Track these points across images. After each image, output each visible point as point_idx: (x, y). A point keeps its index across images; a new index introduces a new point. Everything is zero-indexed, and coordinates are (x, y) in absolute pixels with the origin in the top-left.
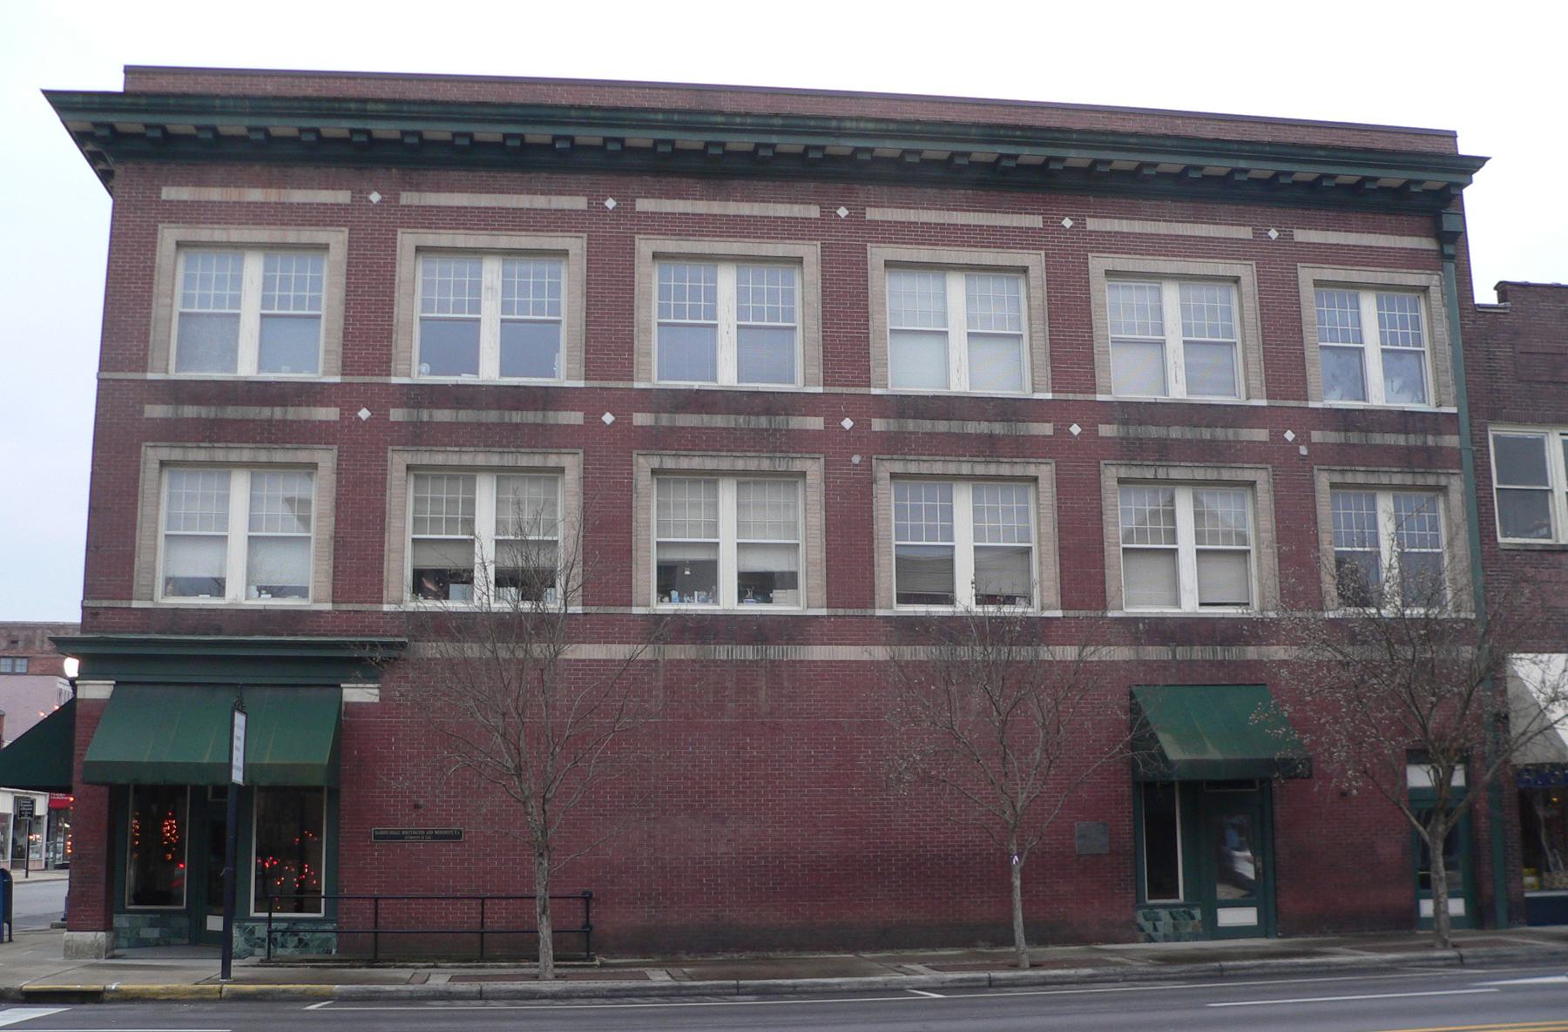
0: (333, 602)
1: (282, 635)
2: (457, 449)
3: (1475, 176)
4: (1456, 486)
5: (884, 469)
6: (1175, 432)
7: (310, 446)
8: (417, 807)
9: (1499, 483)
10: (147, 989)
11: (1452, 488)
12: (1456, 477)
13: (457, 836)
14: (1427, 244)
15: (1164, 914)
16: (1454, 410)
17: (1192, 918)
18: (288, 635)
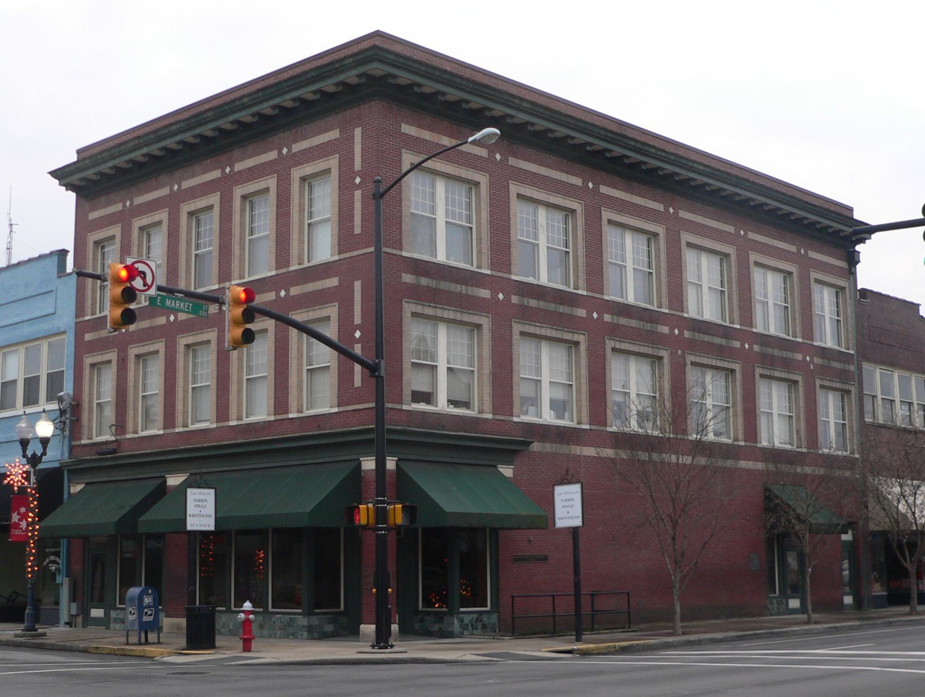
0: (493, 414)
1: (471, 433)
2: (540, 325)
3: (873, 236)
4: (853, 390)
5: (690, 358)
6: (776, 352)
7: (479, 313)
8: (530, 541)
9: (882, 394)
10: (588, 648)
11: (853, 392)
12: (853, 386)
13: (545, 559)
14: (843, 264)
15: (775, 602)
16: (852, 352)
17: (783, 603)
18: (475, 433)
